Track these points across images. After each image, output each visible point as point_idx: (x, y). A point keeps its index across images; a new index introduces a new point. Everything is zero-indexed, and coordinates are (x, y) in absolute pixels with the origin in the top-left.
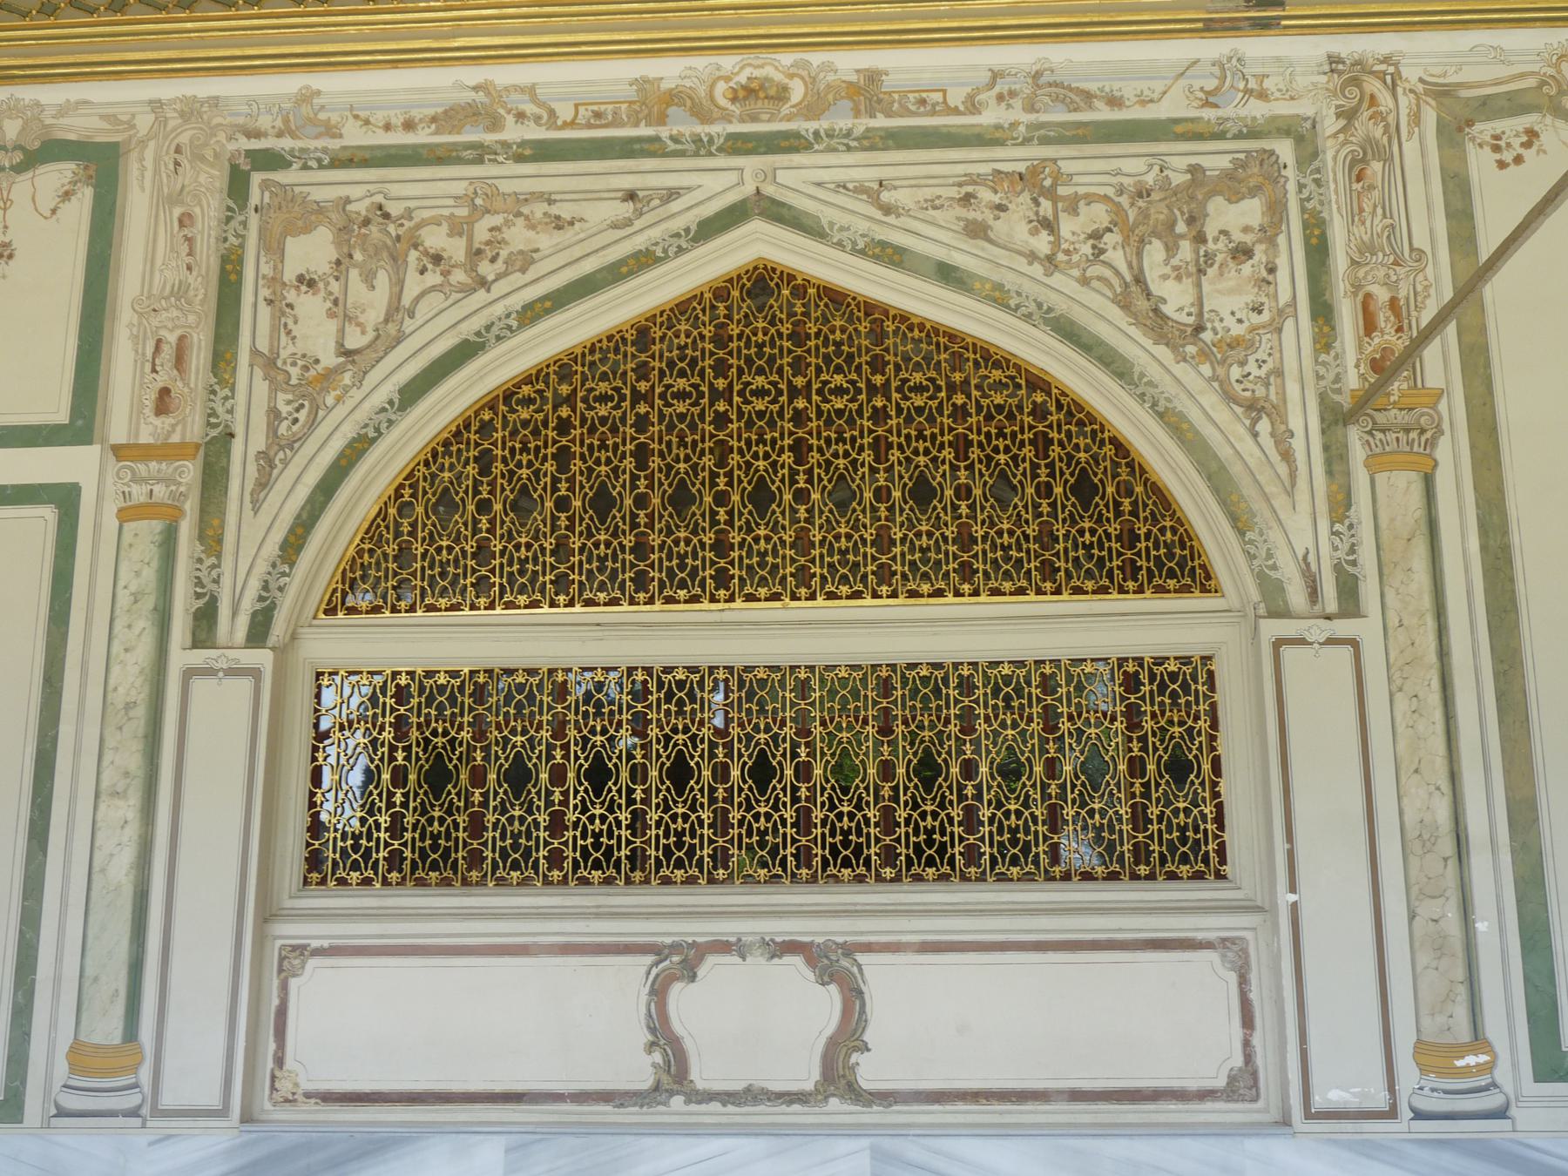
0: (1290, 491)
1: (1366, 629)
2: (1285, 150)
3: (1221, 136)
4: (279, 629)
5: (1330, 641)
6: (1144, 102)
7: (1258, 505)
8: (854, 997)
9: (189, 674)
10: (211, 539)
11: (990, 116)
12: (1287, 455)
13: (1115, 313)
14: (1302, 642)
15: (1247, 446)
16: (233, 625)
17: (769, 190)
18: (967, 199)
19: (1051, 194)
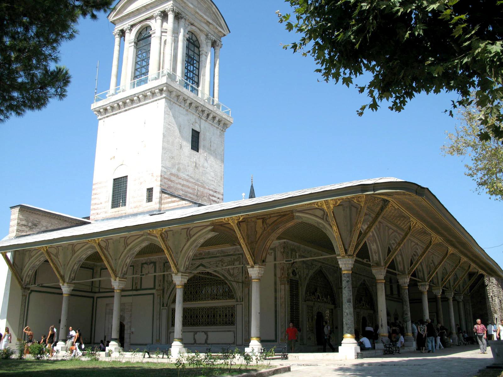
0: (239, 290)
1: (243, 303)
2: (241, 256)
3: (236, 255)
4: (168, 305)
5: (241, 304)
6: (230, 252)
7: (236, 292)
8: (207, 336)
9: (162, 309)
10: (163, 297)
11: (218, 255)
12: (239, 287)
13: (227, 274)
14: (238, 304)
15: (236, 286)
16: (165, 305)
17: (202, 263)
18: (216, 263)
19: (223, 262)
